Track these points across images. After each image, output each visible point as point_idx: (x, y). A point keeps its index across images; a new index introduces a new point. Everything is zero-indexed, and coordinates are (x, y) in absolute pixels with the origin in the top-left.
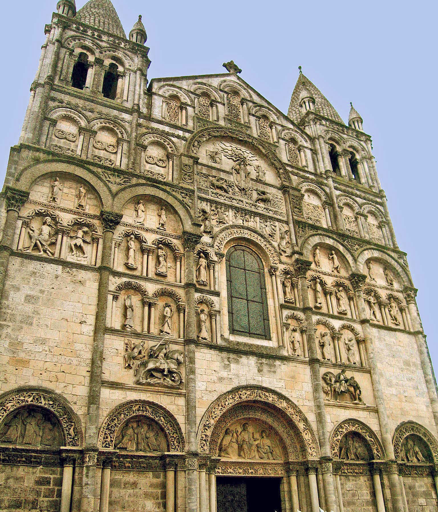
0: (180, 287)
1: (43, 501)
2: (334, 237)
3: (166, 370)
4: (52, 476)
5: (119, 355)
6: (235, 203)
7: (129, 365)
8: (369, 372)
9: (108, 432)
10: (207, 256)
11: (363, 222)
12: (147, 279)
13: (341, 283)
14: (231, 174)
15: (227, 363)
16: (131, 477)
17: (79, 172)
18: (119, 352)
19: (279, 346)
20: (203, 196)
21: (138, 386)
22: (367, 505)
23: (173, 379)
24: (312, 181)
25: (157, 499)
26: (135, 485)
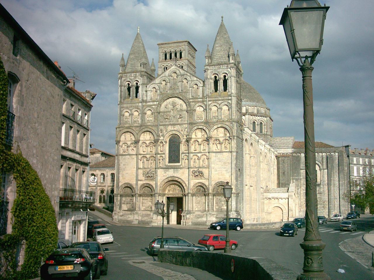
6: (171, 123)
16: (146, 198)
20: (162, 124)
26: (147, 199)
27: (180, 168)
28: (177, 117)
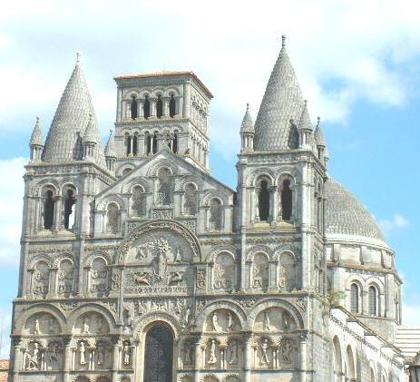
6: (153, 294)
10: (129, 344)
17: (47, 310)
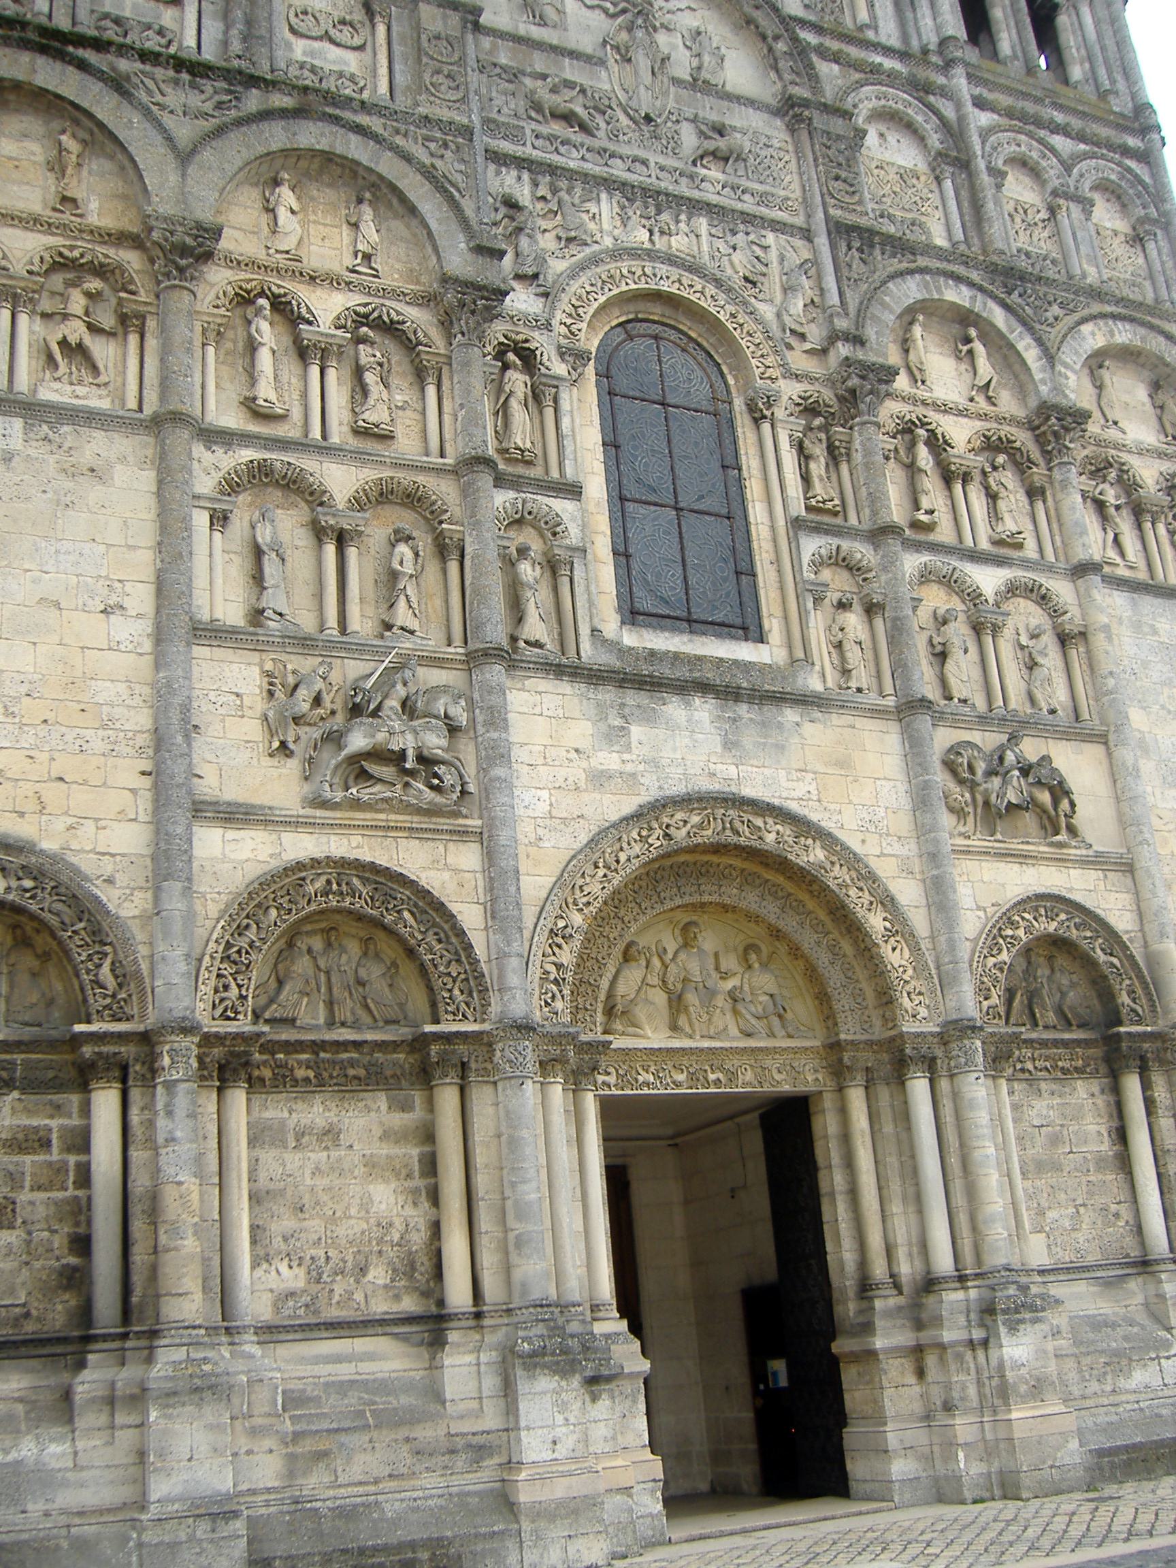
0: (439, 471)
1: (32, 1203)
2: (975, 276)
3: (410, 753)
4: (54, 1123)
5: (248, 713)
6: (618, 170)
7: (283, 744)
8: (1102, 739)
9: (228, 969)
10: (528, 359)
11: (1076, 223)
12: (325, 449)
13: (1000, 439)
14: (602, 62)
15: (618, 722)
18: (247, 701)
19: (793, 661)
20: (506, 146)
21: (318, 813)
22: (1099, 1169)
23: (436, 782)
24: (892, 78)
25: (409, 1176)
26: (330, 1135)
27: (805, 700)
28: (675, 138)
